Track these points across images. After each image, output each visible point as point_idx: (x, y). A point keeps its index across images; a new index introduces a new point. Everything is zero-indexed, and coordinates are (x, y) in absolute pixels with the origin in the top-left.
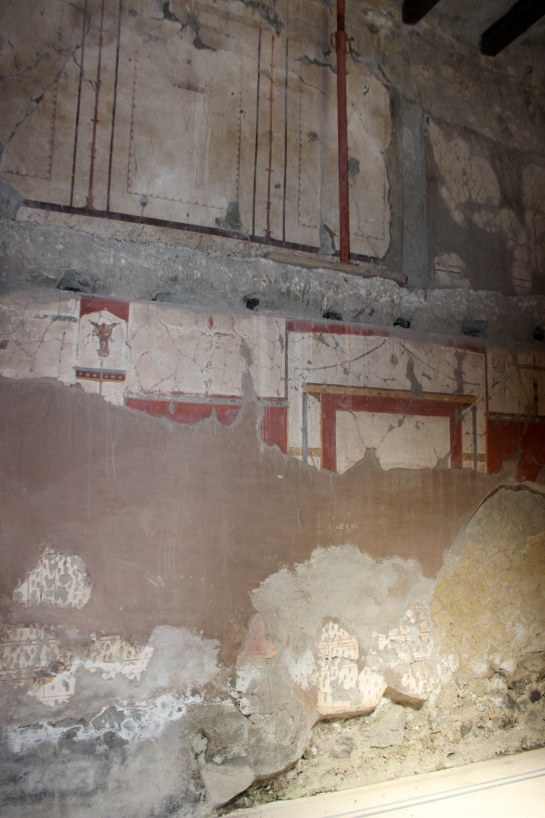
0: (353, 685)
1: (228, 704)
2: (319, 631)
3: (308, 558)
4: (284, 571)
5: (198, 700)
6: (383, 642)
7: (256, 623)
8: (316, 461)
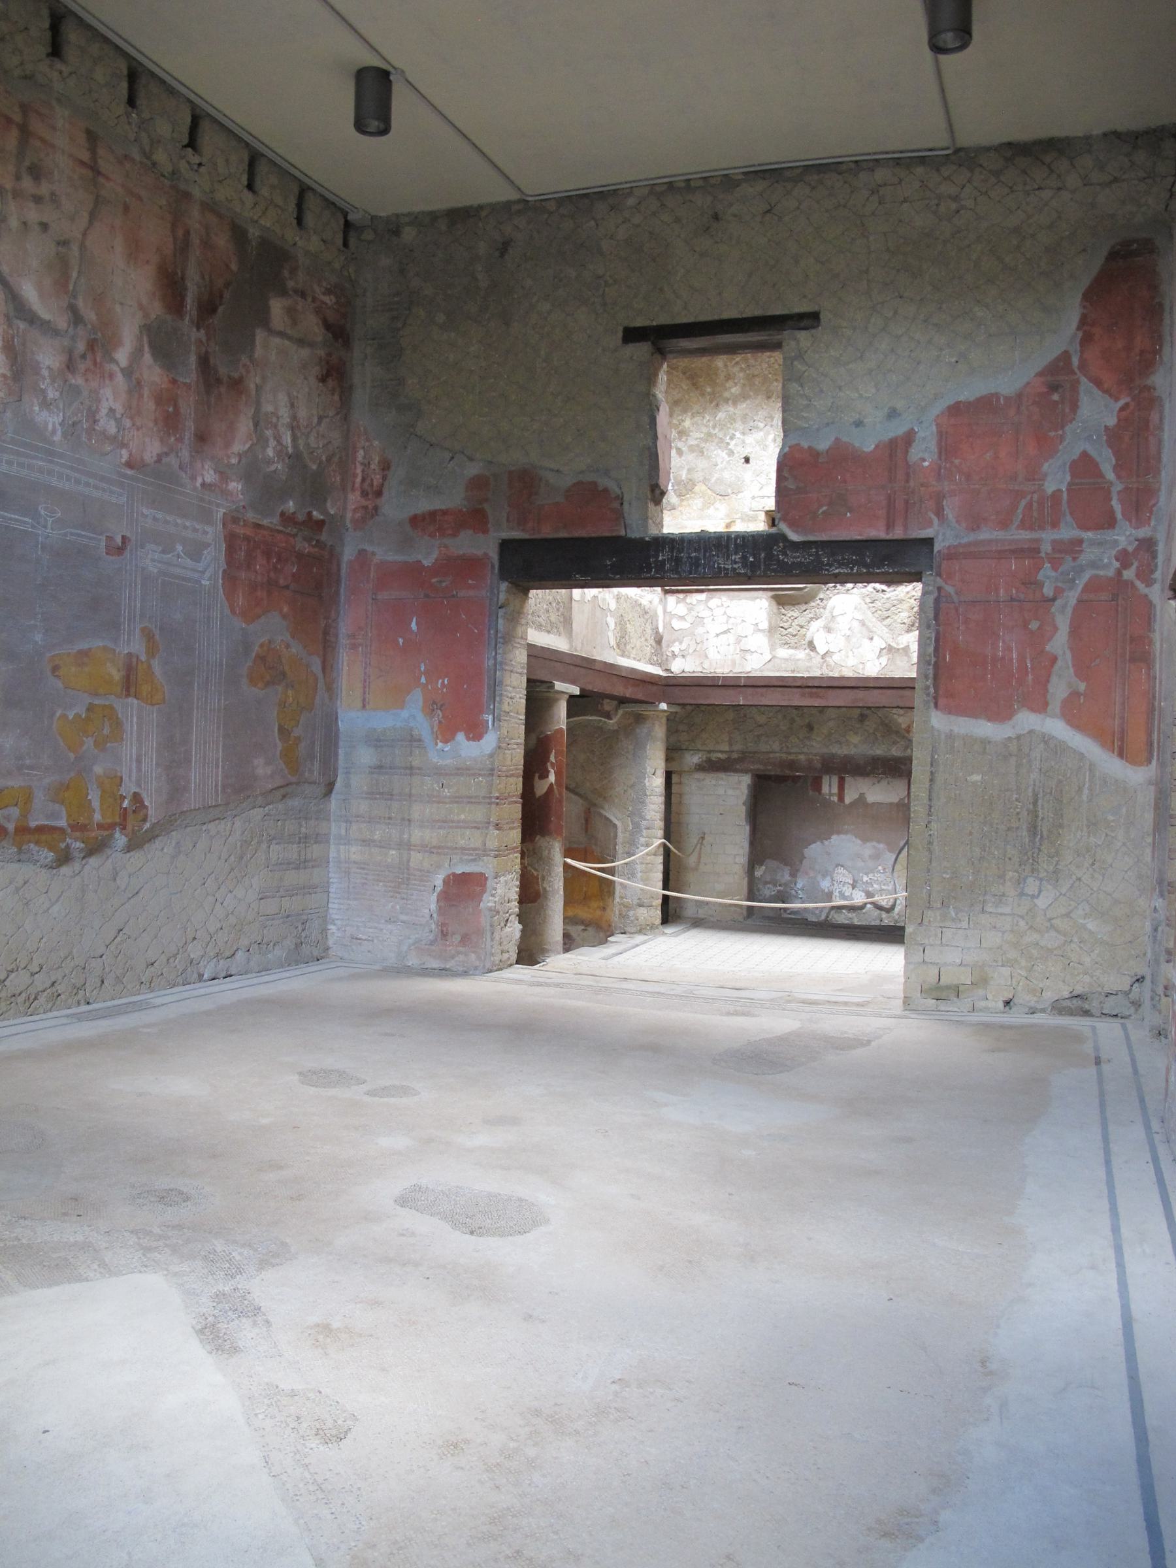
0: (849, 894)
1: (793, 892)
2: (834, 870)
3: (830, 838)
4: (818, 843)
5: (782, 888)
6: (865, 879)
7: (804, 862)
8: (835, 799)
